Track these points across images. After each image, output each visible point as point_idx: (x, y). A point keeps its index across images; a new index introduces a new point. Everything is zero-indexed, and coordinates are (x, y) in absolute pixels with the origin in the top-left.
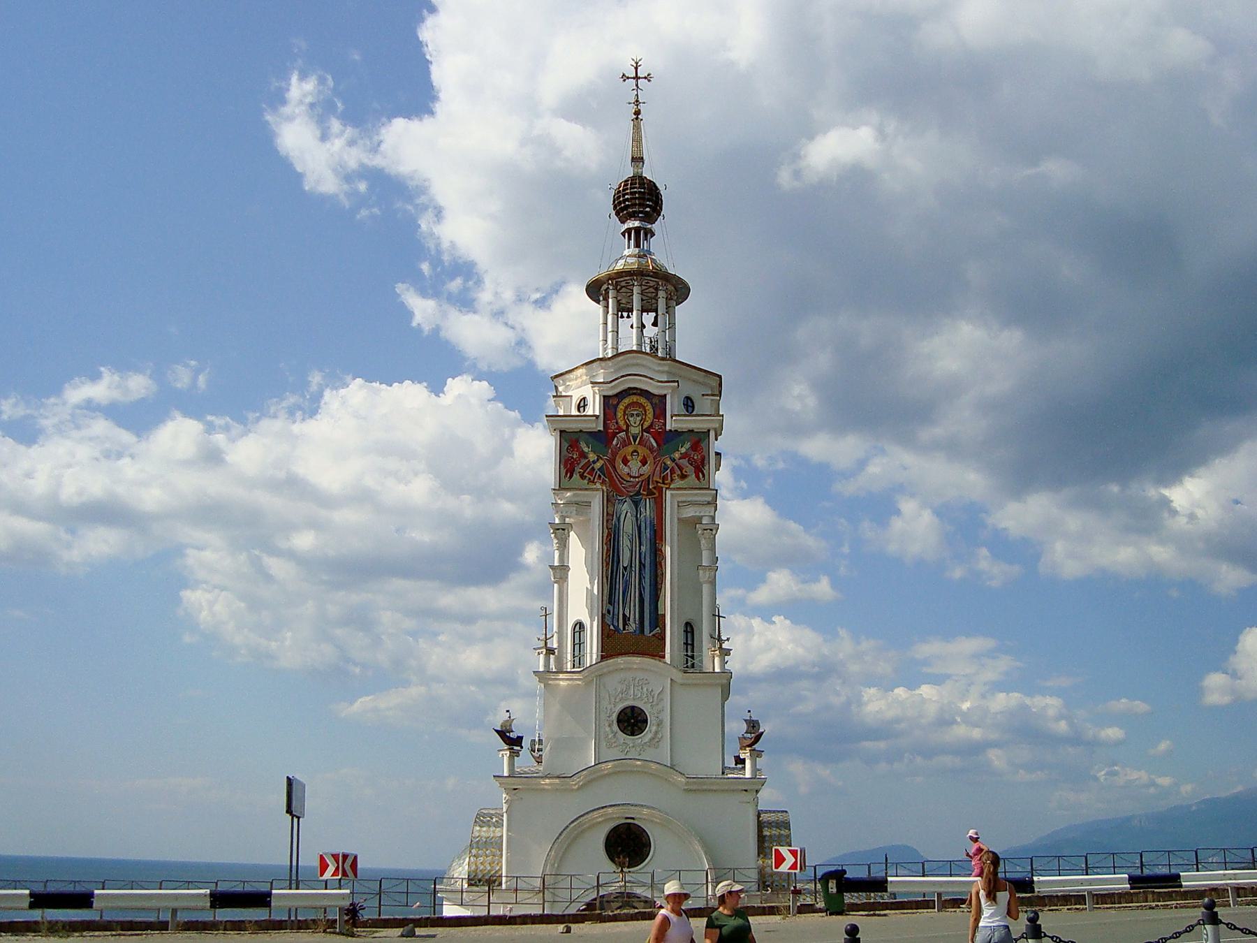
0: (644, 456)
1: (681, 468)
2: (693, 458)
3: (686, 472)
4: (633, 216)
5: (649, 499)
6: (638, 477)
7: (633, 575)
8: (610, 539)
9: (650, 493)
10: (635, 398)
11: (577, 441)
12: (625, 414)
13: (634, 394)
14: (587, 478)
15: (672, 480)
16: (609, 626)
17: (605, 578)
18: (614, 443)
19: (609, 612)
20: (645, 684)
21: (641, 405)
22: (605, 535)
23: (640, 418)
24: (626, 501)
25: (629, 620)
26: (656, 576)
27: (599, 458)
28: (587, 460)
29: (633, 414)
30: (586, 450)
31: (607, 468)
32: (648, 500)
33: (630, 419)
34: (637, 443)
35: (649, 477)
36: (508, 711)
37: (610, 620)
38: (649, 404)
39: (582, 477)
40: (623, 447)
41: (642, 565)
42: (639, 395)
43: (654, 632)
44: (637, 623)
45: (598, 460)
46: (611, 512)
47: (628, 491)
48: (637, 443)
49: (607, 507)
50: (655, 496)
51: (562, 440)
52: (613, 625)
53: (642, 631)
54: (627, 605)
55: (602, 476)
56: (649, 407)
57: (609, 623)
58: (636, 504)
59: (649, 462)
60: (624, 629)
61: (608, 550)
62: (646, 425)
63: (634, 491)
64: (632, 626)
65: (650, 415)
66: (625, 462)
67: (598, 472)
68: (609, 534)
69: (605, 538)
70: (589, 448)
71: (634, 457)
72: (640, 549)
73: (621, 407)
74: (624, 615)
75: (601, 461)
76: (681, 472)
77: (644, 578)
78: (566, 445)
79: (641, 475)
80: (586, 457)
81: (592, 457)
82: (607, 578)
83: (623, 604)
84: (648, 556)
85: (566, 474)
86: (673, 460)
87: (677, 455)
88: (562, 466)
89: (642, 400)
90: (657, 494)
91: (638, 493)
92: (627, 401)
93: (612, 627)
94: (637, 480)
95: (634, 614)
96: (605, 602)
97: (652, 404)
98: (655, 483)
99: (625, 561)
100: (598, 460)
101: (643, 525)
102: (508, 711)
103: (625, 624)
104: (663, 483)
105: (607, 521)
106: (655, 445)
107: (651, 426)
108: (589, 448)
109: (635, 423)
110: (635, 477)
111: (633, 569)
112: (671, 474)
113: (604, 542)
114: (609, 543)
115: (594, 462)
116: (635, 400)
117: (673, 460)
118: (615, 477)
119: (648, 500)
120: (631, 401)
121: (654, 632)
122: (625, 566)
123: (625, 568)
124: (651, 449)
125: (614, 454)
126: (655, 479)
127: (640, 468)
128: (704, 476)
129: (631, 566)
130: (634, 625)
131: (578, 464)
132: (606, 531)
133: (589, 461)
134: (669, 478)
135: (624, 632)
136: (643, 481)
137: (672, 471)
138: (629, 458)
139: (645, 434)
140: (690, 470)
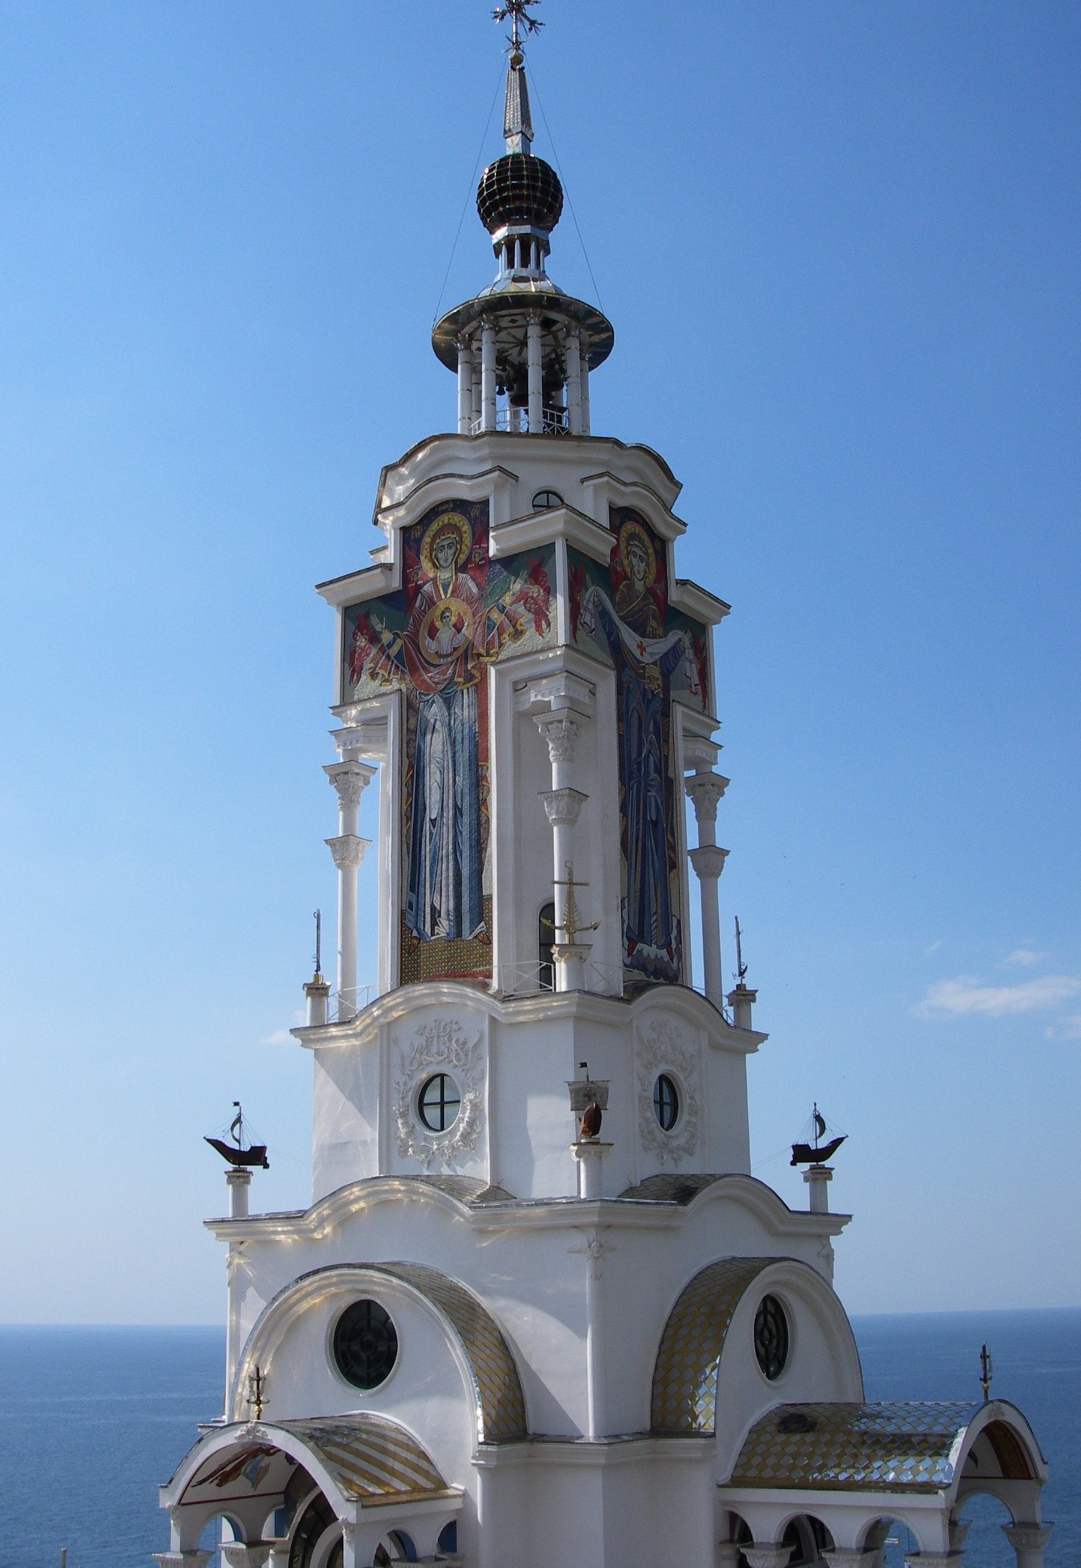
0: (459, 614)
1: (513, 620)
2: (532, 597)
3: (521, 625)
4: (501, 221)
5: (468, 689)
6: (448, 655)
7: (445, 829)
8: (412, 776)
9: (469, 678)
10: (445, 519)
11: (367, 616)
12: (431, 550)
13: (446, 511)
14: (380, 676)
15: (501, 645)
16: (412, 931)
17: (405, 846)
18: (417, 604)
19: (410, 906)
20: (455, 1031)
21: (454, 528)
22: (405, 769)
23: (452, 551)
24: (433, 702)
25: (440, 916)
26: (479, 824)
27: (396, 636)
28: (380, 645)
29: (443, 546)
30: (378, 627)
31: (407, 649)
32: (465, 691)
33: (440, 555)
34: (448, 596)
35: (466, 651)
36: (236, 1104)
37: (413, 919)
38: (466, 521)
39: (373, 675)
40: (429, 608)
41: (458, 810)
42: (453, 510)
43: (477, 931)
44: (451, 918)
45: (394, 640)
46: (412, 727)
47: (437, 683)
48: (448, 596)
49: (408, 719)
50: (474, 682)
51: (347, 620)
52: (416, 927)
53: (459, 933)
54: (437, 889)
55: (401, 667)
56: (466, 528)
57: (411, 926)
58: (448, 703)
59: (466, 624)
60: (433, 934)
61: (409, 795)
62: (463, 557)
63: (446, 679)
64: (444, 927)
65: (468, 539)
66: (433, 632)
67: (395, 661)
68: (411, 767)
69: (405, 774)
70: (382, 624)
71: (444, 620)
72: (454, 780)
73: (427, 539)
74: (433, 907)
75: (398, 640)
76: (514, 626)
77: (461, 833)
78: (352, 627)
79: (455, 649)
80: (379, 640)
81: (387, 637)
82: (408, 844)
83: (431, 888)
84: (466, 790)
85: (352, 676)
86: (502, 610)
87: (507, 599)
88: (347, 665)
89: (457, 519)
90: (478, 675)
91: (451, 682)
92: (435, 526)
93: (415, 933)
94: (450, 659)
95: (446, 904)
96: (405, 889)
97: (469, 519)
98: (475, 658)
99: (433, 812)
100: (394, 640)
101: (459, 737)
102: (236, 1104)
103: (434, 923)
104: (488, 655)
105: (408, 743)
106: (475, 590)
107: (469, 560)
108: (382, 624)
109: (446, 561)
110: (448, 655)
111: (445, 820)
112: (500, 635)
113: (404, 784)
114: (410, 782)
115: (390, 646)
116: (446, 522)
117: (502, 610)
118: (416, 659)
119: (465, 691)
120: (441, 524)
121: (477, 931)
122: (433, 818)
123: (433, 822)
124: (469, 600)
125: (417, 623)
126: (474, 652)
127: (454, 636)
128: (549, 625)
129: (442, 816)
130: (445, 923)
131: (368, 655)
132: (406, 761)
133: (383, 644)
134: (497, 644)
135: (433, 938)
136: (458, 658)
137: (501, 631)
138: (438, 624)
139: (460, 575)
140: (525, 617)
